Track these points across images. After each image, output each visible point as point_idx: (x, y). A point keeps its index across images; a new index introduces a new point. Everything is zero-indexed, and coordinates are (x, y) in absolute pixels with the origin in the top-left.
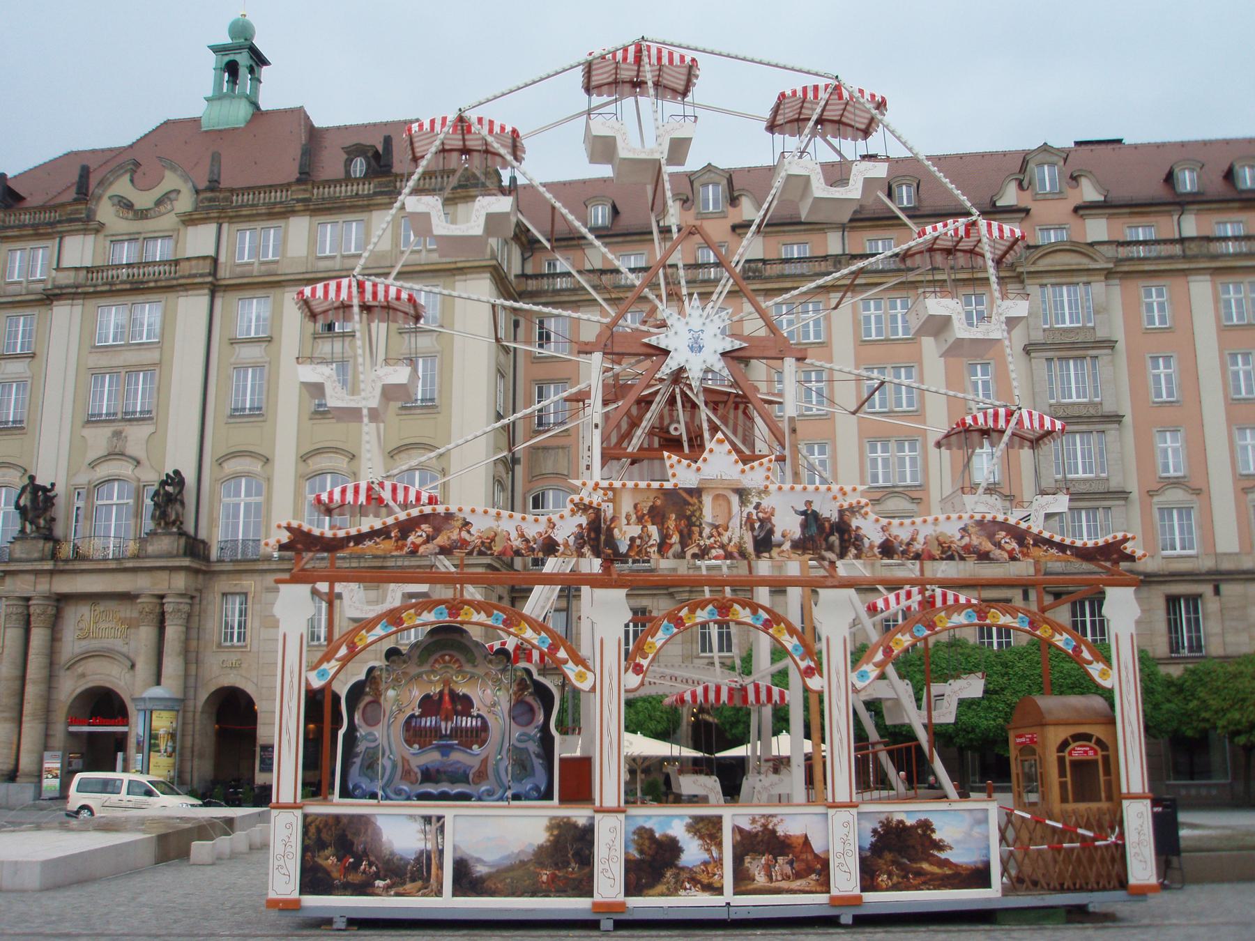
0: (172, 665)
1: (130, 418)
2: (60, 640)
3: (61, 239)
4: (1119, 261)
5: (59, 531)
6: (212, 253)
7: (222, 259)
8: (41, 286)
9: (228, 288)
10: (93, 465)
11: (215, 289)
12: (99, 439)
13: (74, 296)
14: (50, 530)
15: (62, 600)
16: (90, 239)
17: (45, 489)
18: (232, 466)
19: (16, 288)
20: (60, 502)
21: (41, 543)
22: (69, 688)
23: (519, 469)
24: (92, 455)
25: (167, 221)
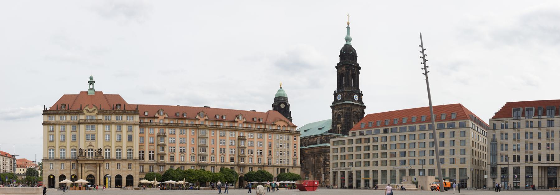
6: (101, 119)
7: (103, 120)
9: (104, 124)
11: (102, 124)
13: (83, 124)
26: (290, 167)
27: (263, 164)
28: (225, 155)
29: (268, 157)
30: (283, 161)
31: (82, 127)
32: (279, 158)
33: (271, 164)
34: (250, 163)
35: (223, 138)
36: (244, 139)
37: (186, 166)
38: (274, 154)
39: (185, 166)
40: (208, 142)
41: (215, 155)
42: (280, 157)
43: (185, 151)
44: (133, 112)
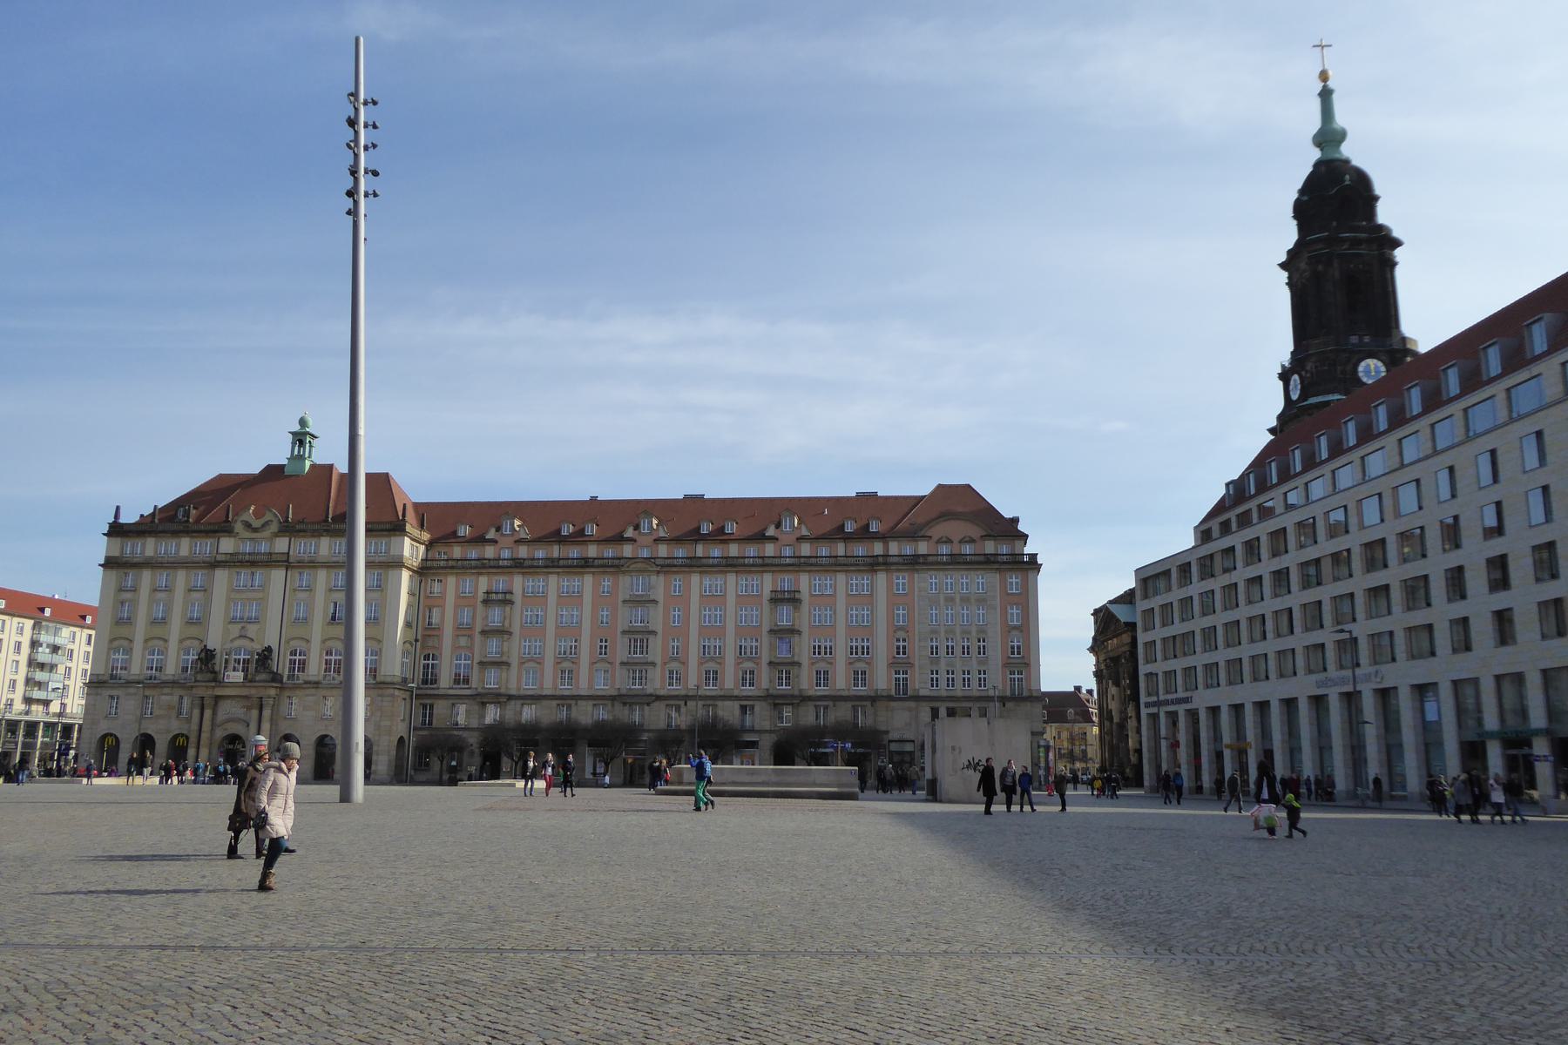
0: (266, 726)
1: (250, 621)
2: (216, 714)
3: (219, 539)
4: (662, 566)
5: (217, 668)
7: (291, 553)
8: (208, 559)
9: (294, 567)
10: (232, 641)
12: (235, 630)
13: (224, 566)
14: (213, 668)
15: (218, 698)
16: (232, 539)
17: (211, 651)
18: (293, 643)
19: (197, 559)
20: (218, 656)
21: (209, 675)
22: (220, 734)
23: (418, 644)
24: (232, 637)
25: (267, 533)
26: (989, 699)
27: (872, 694)
28: (720, 660)
29: (890, 665)
30: (959, 677)
31: (221, 575)
32: (943, 667)
33: (905, 692)
34: (822, 690)
35: (714, 599)
36: (789, 600)
37: (576, 704)
38: (919, 653)
39: (573, 702)
40: (656, 619)
41: (683, 663)
42: (943, 663)
43: (575, 654)
44: (388, 526)
